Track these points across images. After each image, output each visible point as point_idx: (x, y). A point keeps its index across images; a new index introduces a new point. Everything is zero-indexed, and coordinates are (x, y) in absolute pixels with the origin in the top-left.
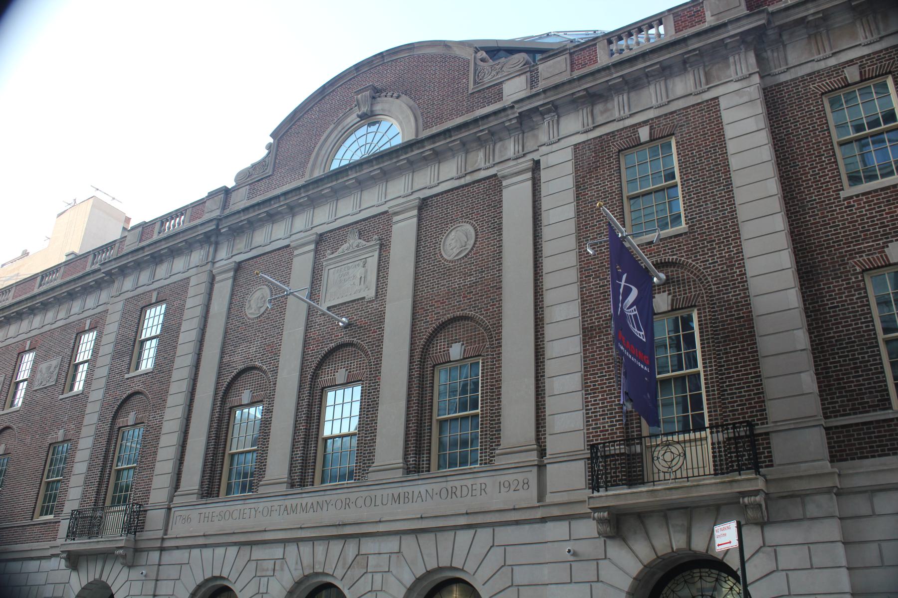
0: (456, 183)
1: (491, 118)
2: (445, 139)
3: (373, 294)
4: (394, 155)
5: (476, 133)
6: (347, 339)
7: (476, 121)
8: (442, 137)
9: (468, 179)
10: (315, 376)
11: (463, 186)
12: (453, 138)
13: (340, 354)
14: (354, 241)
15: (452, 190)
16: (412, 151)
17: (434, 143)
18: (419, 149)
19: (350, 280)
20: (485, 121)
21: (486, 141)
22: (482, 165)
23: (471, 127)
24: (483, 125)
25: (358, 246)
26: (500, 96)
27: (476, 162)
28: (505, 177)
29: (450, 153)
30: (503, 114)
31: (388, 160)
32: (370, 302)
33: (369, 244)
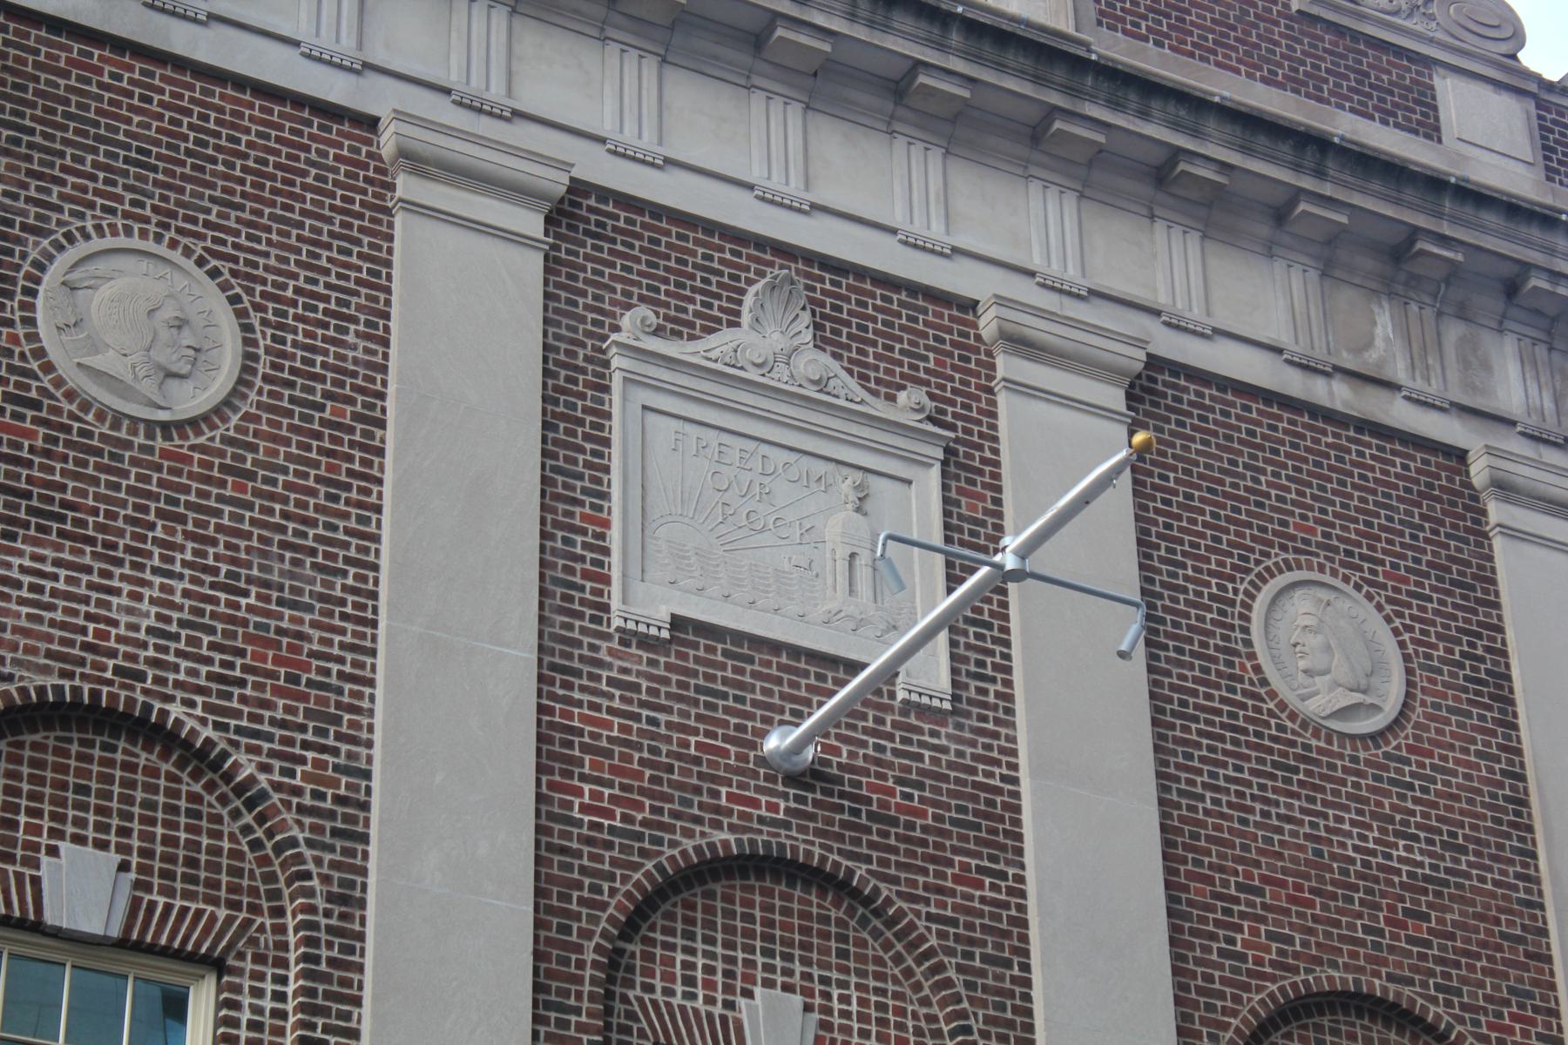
0: (1294, 384)
1: (1491, 218)
2: (1297, 168)
3: (944, 682)
4: (1059, 74)
5: (1415, 232)
6: (806, 845)
7: (1312, 147)
8: (1285, 149)
9: (1337, 395)
10: (614, 965)
11: (1315, 411)
12: (1327, 190)
13: (757, 901)
14: (769, 335)
15: (1269, 396)
16: (1144, 115)
17: (1246, 150)
18: (1176, 126)
19: (776, 533)
20: (1468, 211)
21: (1414, 281)
22: (1399, 371)
23: (1409, 194)
24: (1455, 220)
25: (821, 384)
26: (1430, 129)
27: (1370, 344)
28: (1504, 488)
29: (1264, 230)
30: (1535, 233)
31: (1020, 74)
32: (924, 711)
33: (879, 408)
